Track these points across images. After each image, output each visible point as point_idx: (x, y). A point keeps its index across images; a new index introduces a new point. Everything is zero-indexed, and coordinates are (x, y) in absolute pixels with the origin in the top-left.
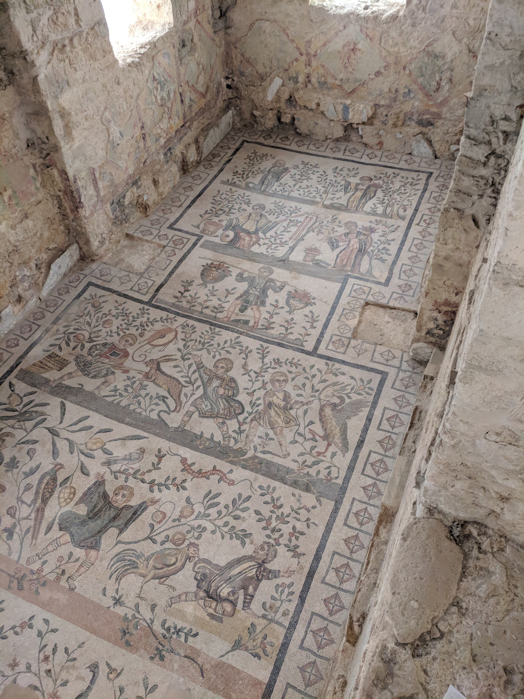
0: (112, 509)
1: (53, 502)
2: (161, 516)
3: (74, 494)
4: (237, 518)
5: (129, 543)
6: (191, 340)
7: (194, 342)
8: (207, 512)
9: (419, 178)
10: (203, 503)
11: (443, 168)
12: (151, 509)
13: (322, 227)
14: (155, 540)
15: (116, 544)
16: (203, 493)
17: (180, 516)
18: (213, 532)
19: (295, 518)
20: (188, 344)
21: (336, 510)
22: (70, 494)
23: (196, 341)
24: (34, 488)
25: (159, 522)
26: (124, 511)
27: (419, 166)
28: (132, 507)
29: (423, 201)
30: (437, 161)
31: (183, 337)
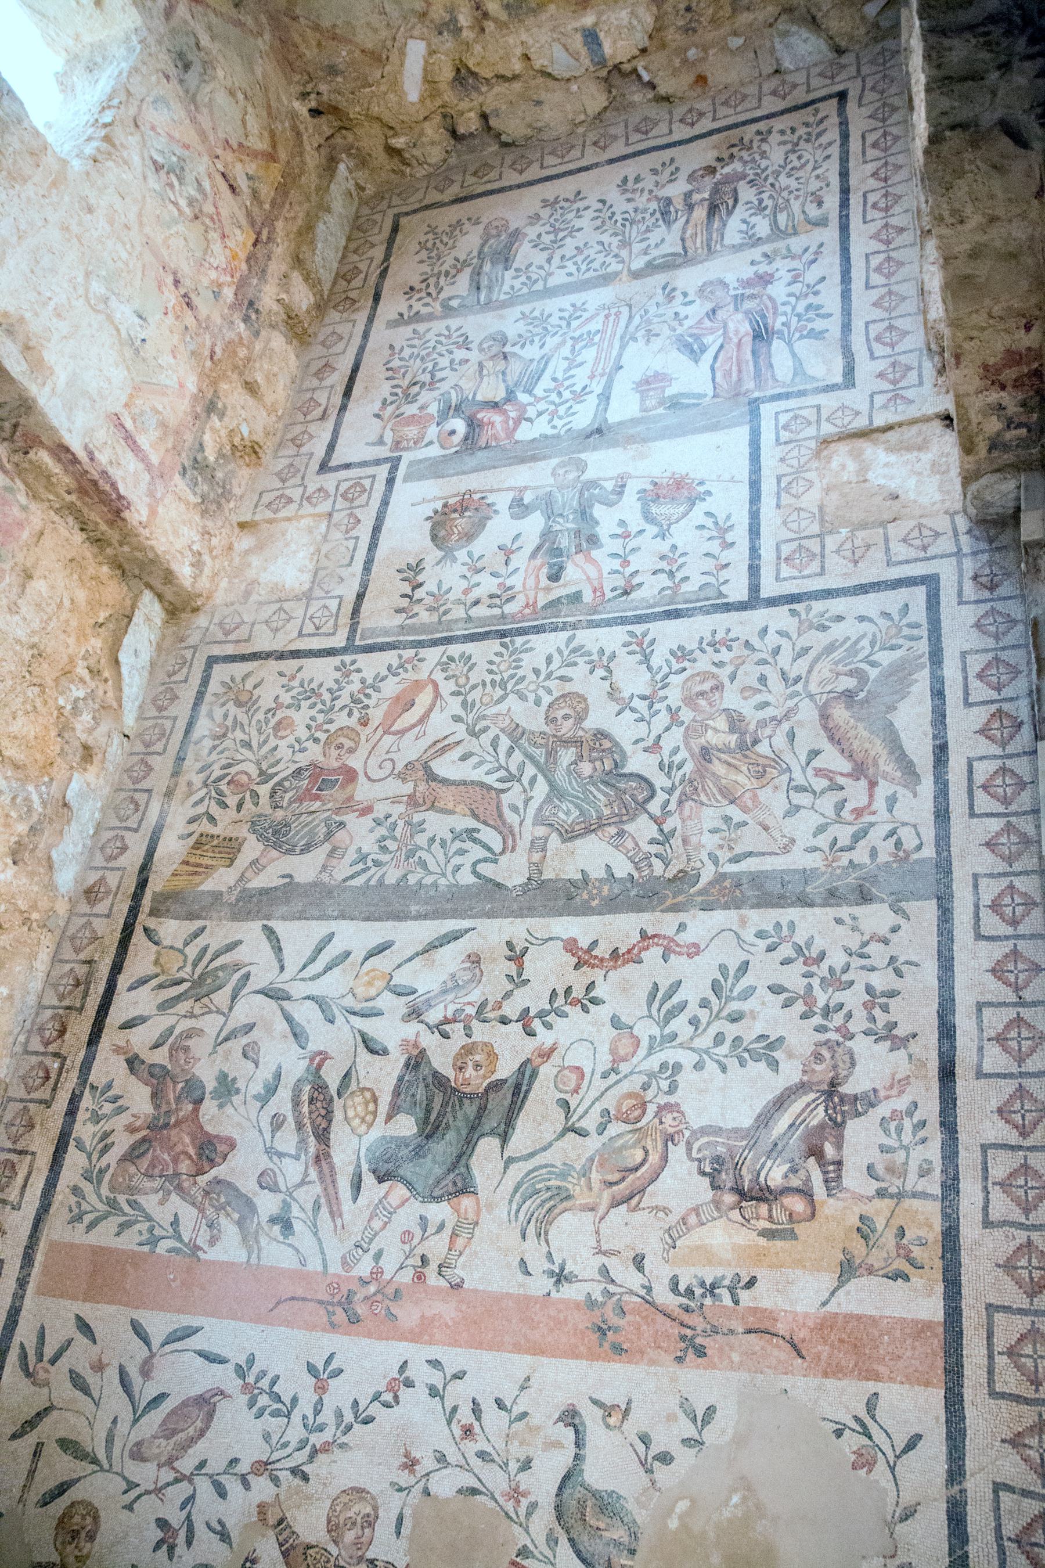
0: (467, 1102)
1: (339, 1133)
2: (573, 1077)
3: (375, 1100)
4: (736, 1018)
5: (532, 1155)
6: (474, 687)
9: (820, 116)
10: (650, 1016)
11: (866, 70)
12: (547, 1071)
13: (649, 322)
15: (506, 1168)
16: (643, 995)
19: (862, 968)
20: (469, 699)
21: (945, 914)
22: (367, 1104)
23: (484, 684)
24: (290, 1119)
25: (576, 1091)
26: (491, 1096)
27: (808, 91)
28: (504, 1081)
29: (852, 164)
30: (845, 60)
31: (454, 688)
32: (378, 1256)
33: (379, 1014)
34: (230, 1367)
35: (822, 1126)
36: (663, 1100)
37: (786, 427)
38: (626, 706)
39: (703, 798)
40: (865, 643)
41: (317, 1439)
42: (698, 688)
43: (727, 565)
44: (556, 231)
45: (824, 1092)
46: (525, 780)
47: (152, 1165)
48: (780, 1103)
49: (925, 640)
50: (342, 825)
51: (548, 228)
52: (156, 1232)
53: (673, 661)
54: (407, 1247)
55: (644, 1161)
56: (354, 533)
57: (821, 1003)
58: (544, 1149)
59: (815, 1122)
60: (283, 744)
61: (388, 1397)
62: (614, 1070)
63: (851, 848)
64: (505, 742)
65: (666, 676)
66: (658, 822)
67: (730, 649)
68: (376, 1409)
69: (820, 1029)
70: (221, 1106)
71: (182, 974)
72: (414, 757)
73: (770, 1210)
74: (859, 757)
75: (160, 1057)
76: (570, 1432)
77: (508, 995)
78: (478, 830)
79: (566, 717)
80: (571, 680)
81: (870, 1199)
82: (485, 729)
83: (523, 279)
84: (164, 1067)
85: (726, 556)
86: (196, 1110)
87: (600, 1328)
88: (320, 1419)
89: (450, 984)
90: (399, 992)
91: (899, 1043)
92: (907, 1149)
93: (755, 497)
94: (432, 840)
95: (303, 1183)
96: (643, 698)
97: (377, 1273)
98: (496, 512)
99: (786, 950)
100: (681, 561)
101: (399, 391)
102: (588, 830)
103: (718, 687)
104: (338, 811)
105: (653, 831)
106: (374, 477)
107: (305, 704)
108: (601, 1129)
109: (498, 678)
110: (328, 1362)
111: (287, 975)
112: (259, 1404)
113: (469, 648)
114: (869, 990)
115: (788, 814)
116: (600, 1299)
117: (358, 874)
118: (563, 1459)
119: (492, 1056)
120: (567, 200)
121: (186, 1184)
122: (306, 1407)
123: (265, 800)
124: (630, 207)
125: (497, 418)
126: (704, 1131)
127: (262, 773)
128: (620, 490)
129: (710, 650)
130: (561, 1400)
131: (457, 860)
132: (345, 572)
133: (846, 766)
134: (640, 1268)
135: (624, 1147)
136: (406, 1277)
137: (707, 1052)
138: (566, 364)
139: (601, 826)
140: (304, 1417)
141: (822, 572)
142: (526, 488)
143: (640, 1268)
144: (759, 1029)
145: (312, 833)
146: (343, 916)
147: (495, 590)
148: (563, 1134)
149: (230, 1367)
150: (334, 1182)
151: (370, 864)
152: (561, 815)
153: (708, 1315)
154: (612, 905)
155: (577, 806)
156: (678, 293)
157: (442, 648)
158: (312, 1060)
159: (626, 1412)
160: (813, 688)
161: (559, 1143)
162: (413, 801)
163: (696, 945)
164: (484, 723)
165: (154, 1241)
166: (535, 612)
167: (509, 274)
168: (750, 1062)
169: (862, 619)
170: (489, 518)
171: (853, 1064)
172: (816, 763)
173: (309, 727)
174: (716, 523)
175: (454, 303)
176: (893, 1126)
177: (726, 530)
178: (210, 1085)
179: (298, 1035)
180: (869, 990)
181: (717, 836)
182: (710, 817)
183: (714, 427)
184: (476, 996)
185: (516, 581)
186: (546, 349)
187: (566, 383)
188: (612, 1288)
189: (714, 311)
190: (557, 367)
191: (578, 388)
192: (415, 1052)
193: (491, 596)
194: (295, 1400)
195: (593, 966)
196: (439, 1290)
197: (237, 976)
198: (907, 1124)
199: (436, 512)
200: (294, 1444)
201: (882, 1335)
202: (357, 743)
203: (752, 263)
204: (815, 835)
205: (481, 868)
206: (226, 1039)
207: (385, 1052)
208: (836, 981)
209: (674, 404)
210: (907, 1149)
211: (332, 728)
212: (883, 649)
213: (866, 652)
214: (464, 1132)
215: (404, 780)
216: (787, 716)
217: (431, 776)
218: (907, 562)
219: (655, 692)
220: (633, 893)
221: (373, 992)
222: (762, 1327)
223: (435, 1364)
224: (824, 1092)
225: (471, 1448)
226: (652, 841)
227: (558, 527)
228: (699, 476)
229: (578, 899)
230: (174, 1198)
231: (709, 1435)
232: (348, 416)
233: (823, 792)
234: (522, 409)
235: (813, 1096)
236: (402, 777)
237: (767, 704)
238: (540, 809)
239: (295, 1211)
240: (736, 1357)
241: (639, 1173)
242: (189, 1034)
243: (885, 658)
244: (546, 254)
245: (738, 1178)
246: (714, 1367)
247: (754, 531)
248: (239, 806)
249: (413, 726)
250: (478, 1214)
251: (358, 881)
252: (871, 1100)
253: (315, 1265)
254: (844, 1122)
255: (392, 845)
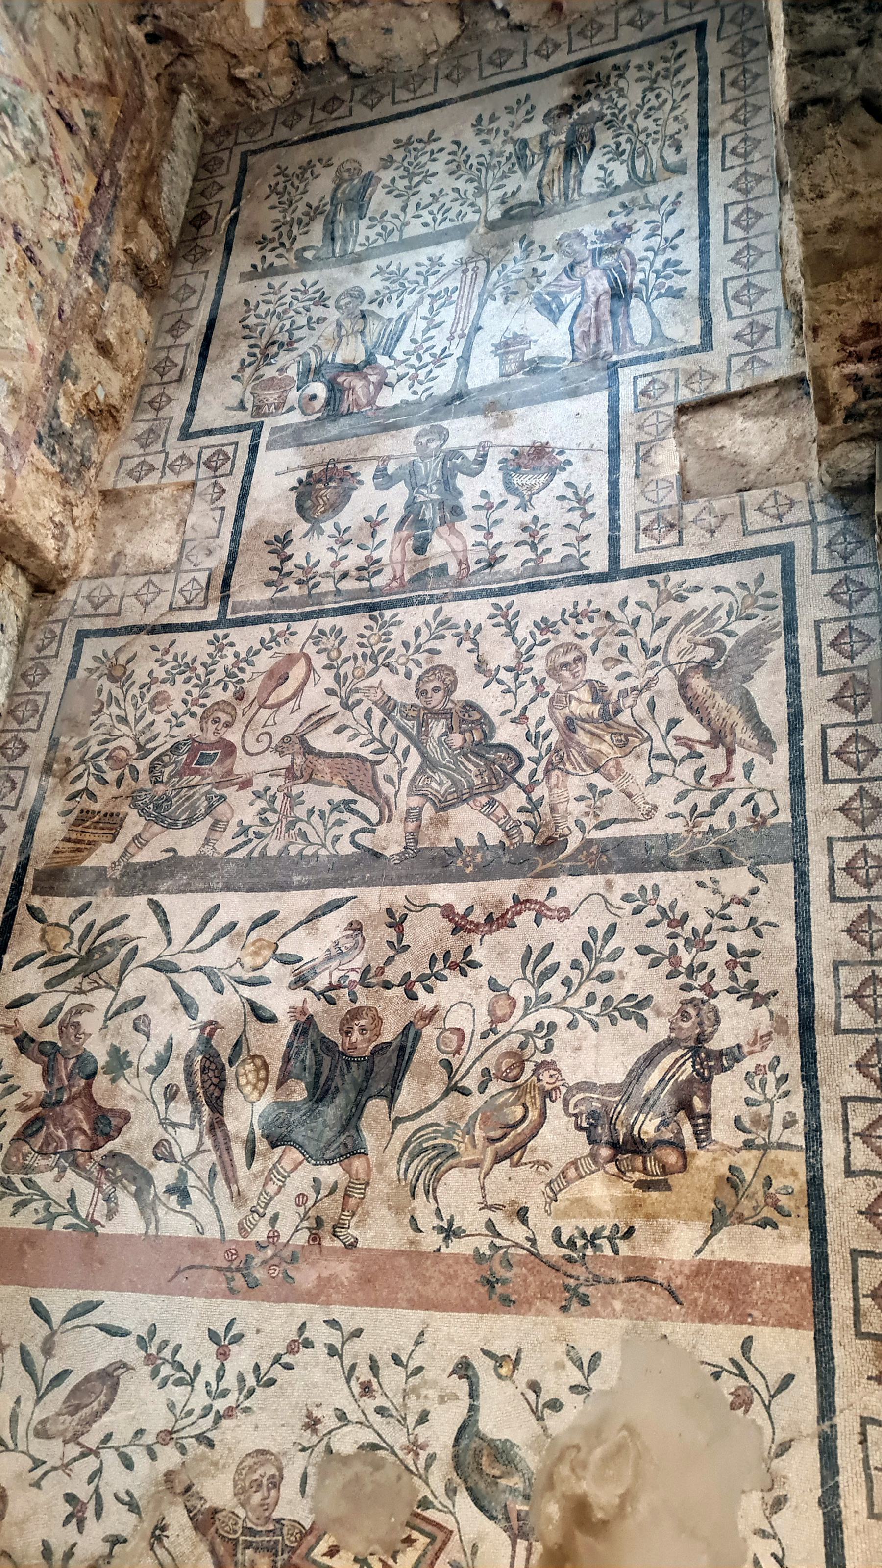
0: (354, 1065)
1: (232, 1100)
2: (455, 1038)
3: (266, 1066)
4: (606, 977)
6: (346, 660)
7: (352, 661)
8: (541, 992)
14: (463, 1088)
16: (516, 958)
17: (492, 1022)
18: (572, 1025)
19: (724, 929)
20: (342, 672)
21: (802, 879)
22: (257, 1070)
23: (355, 658)
24: (183, 1089)
25: (457, 1051)
28: (390, 1044)
31: (326, 662)
32: (275, 1219)
33: (267, 982)
34: (132, 1339)
35: (690, 1081)
36: (539, 1058)
37: (644, 393)
38: (492, 678)
39: (569, 767)
40: (722, 613)
41: (220, 1405)
42: (562, 660)
43: (587, 537)
44: (410, 176)
45: (690, 1048)
46: (399, 752)
47: (46, 1143)
48: (650, 1059)
49: (780, 610)
50: (223, 798)
51: (401, 172)
52: (52, 1210)
53: (538, 633)
54: (302, 1210)
55: (524, 1117)
56: (220, 504)
57: (686, 962)
58: (429, 1108)
59: (683, 1077)
60: (160, 719)
61: (286, 1359)
62: (493, 1031)
63: (710, 814)
64: (378, 715)
65: (531, 648)
66: (527, 790)
67: (591, 620)
68: (277, 1372)
69: (686, 988)
70: (113, 1081)
71: (69, 951)
72: (291, 731)
73: (644, 1162)
74: (717, 725)
75: (50, 1034)
76: (464, 1385)
77: (390, 960)
78: (355, 802)
79: (436, 690)
80: (439, 652)
81: (738, 1150)
82: (359, 702)
83: (378, 229)
84: (54, 1044)
85: (587, 527)
86: (89, 1086)
87: (488, 1281)
88: (223, 1385)
89: (334, 952)
90: (285, 960)
91: (760, 1001)
92: (771, 1102)
93: (614, 468)
94: (311, 812)
95: (198, 1152)
96: (509, 669)
97: (274, 1237)
98: (360, 482)
99: (651, 913)
100: (542, 533)
101: (257, 351)
102: (461, 800)
103: (581, 659)
104: (218, 785)
105: (521, 799)
106: (237, 444)
107: (180, 679)
108: (483, 1088)
109: (368, 651)
110: (229, 1328)
111: (175, 948)
112: (163, 1374)
113: (340, 621)
114: (731, 949)
115: (650, 781)
116: (488, 1253)
117: (240, 846)
118: (458, 1411)
119: (378, 1021)
120: (420, 141)
121: (81, 1160)
122: (208, 1374)
123: (144, 776)
124: (485, 149)
125: (358, 384)
126: (581, 1087)
127: (140, 747)
128: (482, 460)
129: (572, 621)
130: (455, 1354)
131: (336, 831)
132: (213, 544)
133: (705, 735)
134: (524, 1221)
135: (505, 1104)
136: (302, 1238)
137: (579, 1011)
138: (423, 324)
139: (473, 795)
140: (208, 1384)
141: (680, 543)
142: (389, 458)
143: (524, 1221)
144: (628, 989)
145: (194, 808)
146: (228, 888)
147: (362, 562)
148: (446, 1094)
149: (132, 1339)
150: (229, 1149)
151: (251, 835)
152: (434, 785)
153: (590, 1266)
154: (485, 872)
155: (448, 776)
156: (536, 246)
157: (312, 622)
158: (203, 1029)
159: (517, 1362)
160: (672, 658)
161: (443, 1103)
162: (291, 774)
163: (565, 909)
164: (357, 696)
165: (51, 1218)
166: (402, 585)
167: (364, 223)
168: (621, 1022)
169: (718, 589)
170: (354, 489)
171: (718, 1021)
172: (674, 732)
173: (185, 702)
174: (576, 494)
175: (309, 255)
176: (757, 1080)
177: (586, 501)
178: (102, 1059)
179: (188, 1006)
180: (731, 949)
181: (583, 804)
182: (575, 785)
183: (574, 393)
184: (359, 962)
185: (382, 554)
186: (404, 308)
187: (426, 345)
188: (498, 1242)
189: (572, 267)
190: (416, 326)
191: (437, 351)
192: (303, 1019)
193: (360, 569)
194: (197, 1368)
195: (470, 931)
196: (334, 1250)
197: (124, 951)
198: (771, 1077)
199: (300, 481)
200: (198, 1412)
201: (754, 1281)
202: (234, 717)
203: (610, 214)
204: (676, 802)
205: (362, 839)
206: (117, 1013)
207: (273, 1019)
208: (698, 941)
209: (534, 368)
210: (771, 1102)
211: (208, 702)
212: (739, 618)
213: (723, 622)
214: (352, 1095)
215: (282, 754)
216: (647, 686)
217: (308, 750)
218: (763, 531)
219: (519, 663)
220: (505, 860)
221: (259, 961)
222: (642, 1275)
223: (333, 1323)
224: (690, 1048)
225: (371, 1405)
226: (521, 810)
227: (421, 499)
228: (559, 445)
229: (453, 867)
230: (70, 1174)
231: (595, 1382)
232: (206, 379)
233: (682, 760)
234: (383, 373)
235: (680, 1052)
236: (280, 751)
237: (627, 675)
238: (414, 780)
239: (192, 1180)
240: (618, 1305)
241: (520, 1130)
242: (79, 1010)
243: (742, 628)
244: (400, 202)
245: (613, 1131)
246: (598, 1315)
247: (614, 501)
248: (119, 782)
249: (289, 700)
250: (368, 1175)
251: (241, 854)
252: (735, 1055)
253: (212, 1232)
254: (711, 1077)
255: (272, 817)
